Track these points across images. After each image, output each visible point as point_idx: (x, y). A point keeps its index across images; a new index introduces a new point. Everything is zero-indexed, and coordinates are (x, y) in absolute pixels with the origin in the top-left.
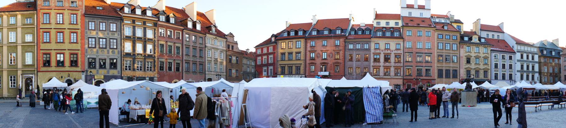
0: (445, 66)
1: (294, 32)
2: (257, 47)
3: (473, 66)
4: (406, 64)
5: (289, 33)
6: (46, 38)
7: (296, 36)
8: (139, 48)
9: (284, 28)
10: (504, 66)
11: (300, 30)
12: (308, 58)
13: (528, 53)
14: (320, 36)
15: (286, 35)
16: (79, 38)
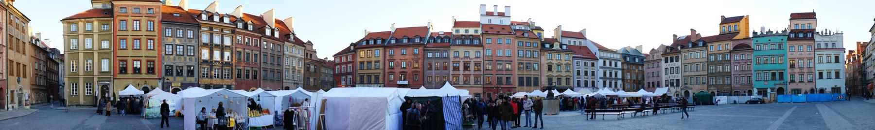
0: (526, 74)
1: (373, 41)
2: (335, 56)
3: (554, 73)
4: (486, 72)
5: (368, 42)
6: (123, 44)
7: (375, 46)
8: (217, 55)
9: (362, 36)
10: (586, 73)
11: (378, 38)
12: (387, 67)
13: (611, 60)
14: (399, 44)
15: (364, 43)
16: (156, 45)
